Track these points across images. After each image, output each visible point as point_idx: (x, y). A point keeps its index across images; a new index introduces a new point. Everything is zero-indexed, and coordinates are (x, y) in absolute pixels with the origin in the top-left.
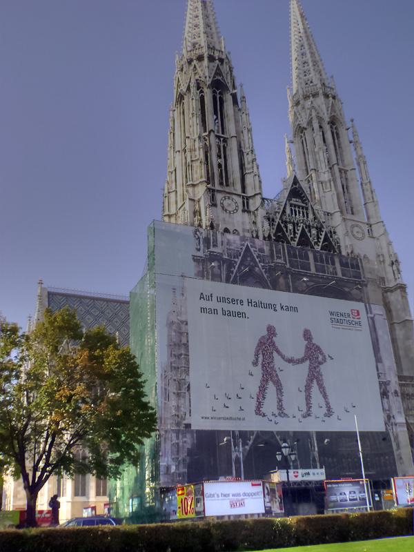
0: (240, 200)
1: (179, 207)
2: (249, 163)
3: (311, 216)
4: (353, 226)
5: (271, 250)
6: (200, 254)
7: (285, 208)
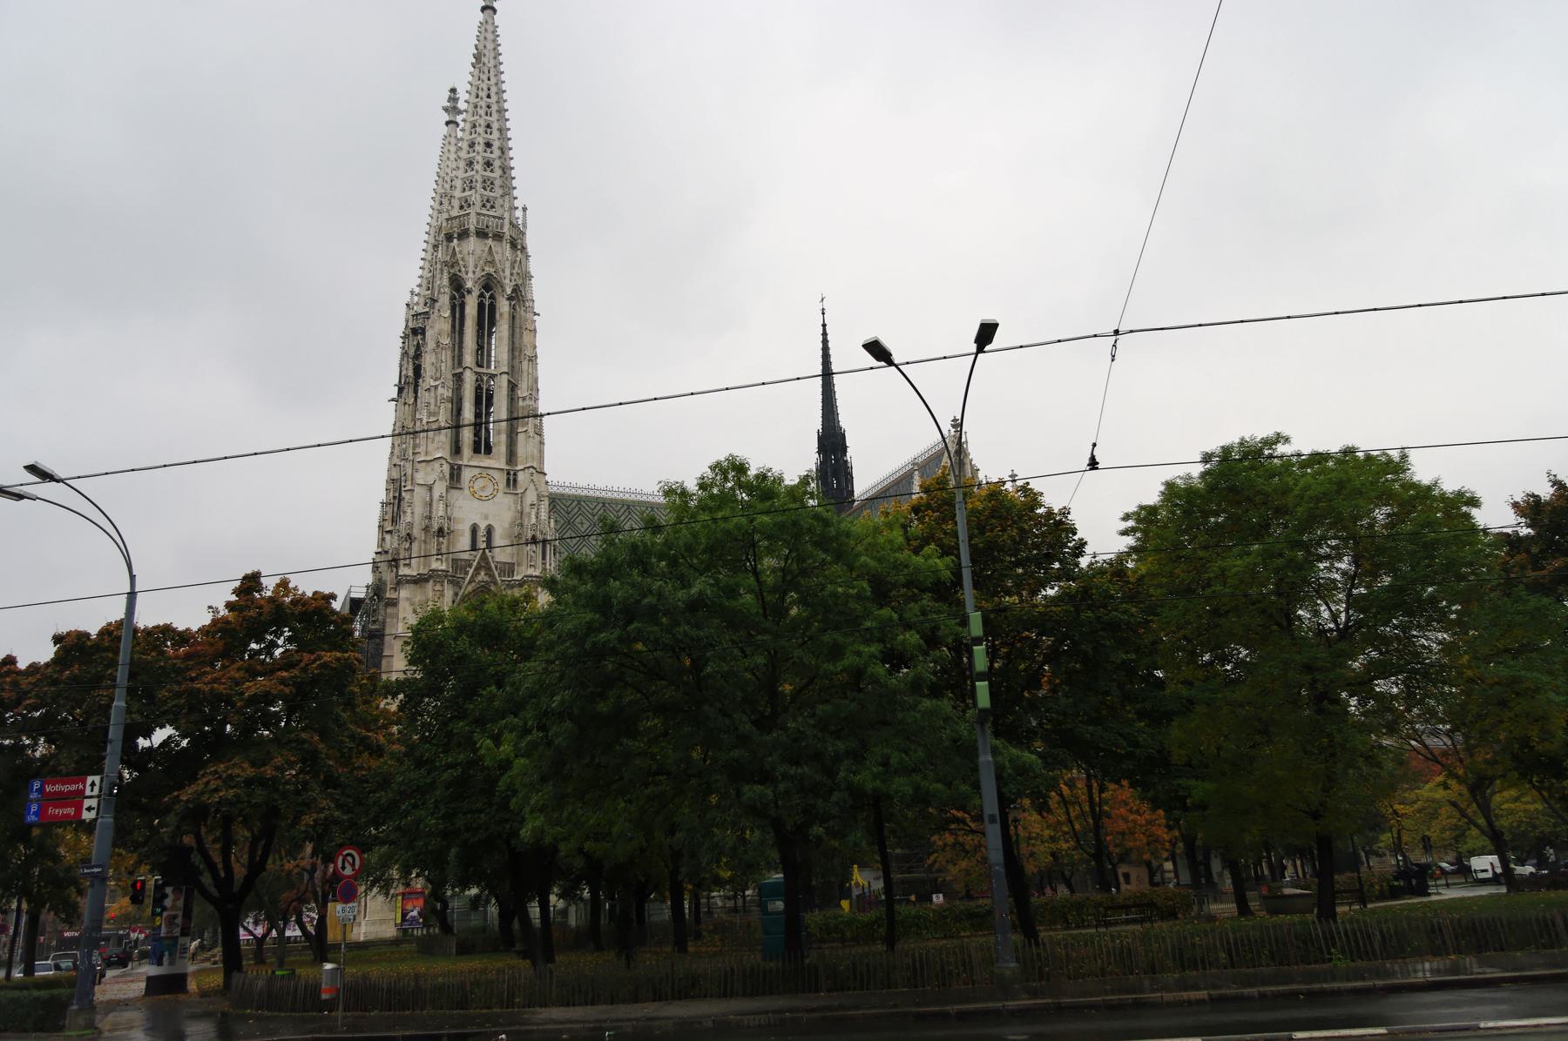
4: (474, 479)
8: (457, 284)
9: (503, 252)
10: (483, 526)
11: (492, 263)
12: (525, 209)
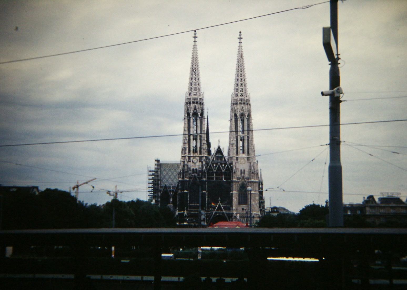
0: (198, 158)
3: (223, 159)
7: (213, 158)
8: (236, 115)
9: (245, 107)
10: (243, 171)
11: (243, 110)
12: (250, 94)
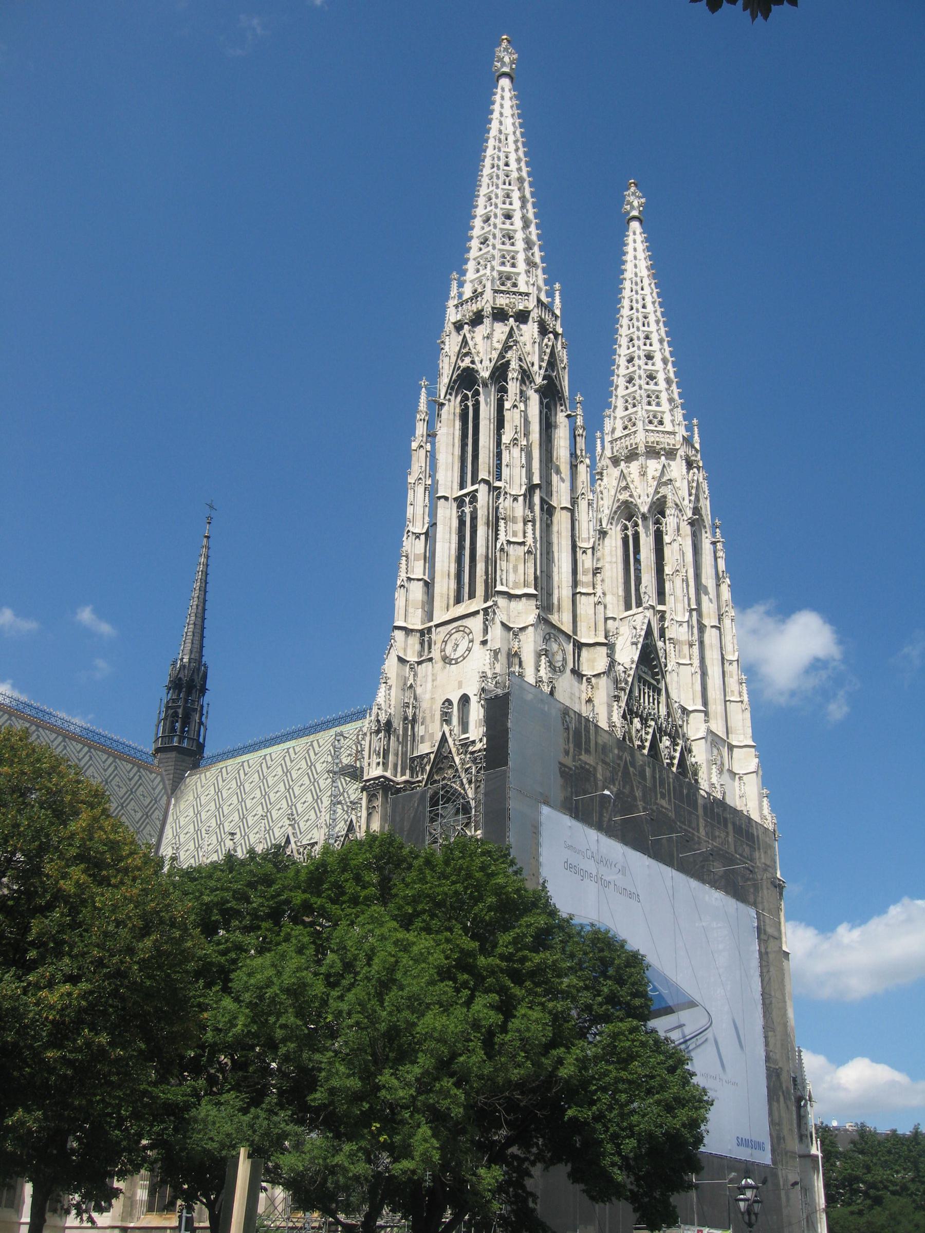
1: (436, 621)
2: (585, 572)
5: (654, 777)
6: (568, 761)
